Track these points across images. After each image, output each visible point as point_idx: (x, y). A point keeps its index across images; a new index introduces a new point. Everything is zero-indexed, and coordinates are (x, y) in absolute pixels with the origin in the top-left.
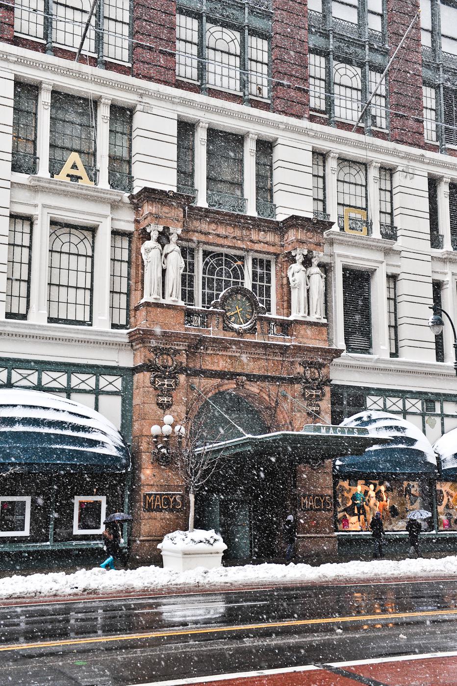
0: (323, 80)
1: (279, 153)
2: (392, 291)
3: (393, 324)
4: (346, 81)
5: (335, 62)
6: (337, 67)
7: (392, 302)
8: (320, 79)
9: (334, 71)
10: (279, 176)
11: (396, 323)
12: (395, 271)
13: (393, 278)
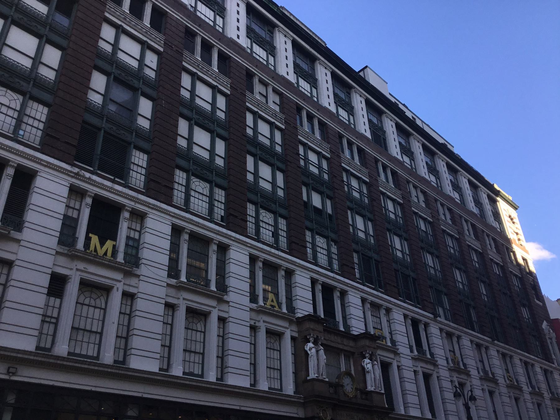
0: (144, 168)
1: (40, 182)
2: (221, 330)
3: (220, 355)
4: (200, 190)
5: (192, 177)
6: (194, 180)
7: (221, 339)
8: (142, 167)
9: (192, 182)
10: (35, 199)
11: (223, 354)
12: (132, 290)
13: (129, 297)
